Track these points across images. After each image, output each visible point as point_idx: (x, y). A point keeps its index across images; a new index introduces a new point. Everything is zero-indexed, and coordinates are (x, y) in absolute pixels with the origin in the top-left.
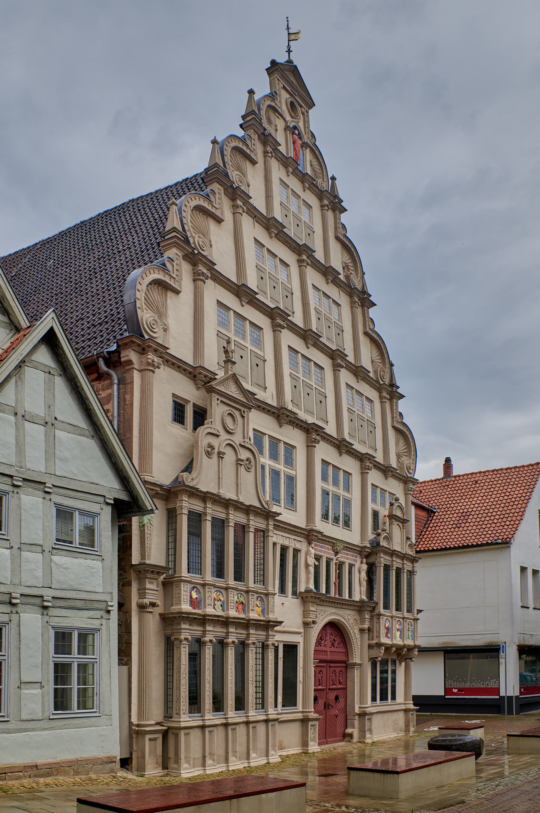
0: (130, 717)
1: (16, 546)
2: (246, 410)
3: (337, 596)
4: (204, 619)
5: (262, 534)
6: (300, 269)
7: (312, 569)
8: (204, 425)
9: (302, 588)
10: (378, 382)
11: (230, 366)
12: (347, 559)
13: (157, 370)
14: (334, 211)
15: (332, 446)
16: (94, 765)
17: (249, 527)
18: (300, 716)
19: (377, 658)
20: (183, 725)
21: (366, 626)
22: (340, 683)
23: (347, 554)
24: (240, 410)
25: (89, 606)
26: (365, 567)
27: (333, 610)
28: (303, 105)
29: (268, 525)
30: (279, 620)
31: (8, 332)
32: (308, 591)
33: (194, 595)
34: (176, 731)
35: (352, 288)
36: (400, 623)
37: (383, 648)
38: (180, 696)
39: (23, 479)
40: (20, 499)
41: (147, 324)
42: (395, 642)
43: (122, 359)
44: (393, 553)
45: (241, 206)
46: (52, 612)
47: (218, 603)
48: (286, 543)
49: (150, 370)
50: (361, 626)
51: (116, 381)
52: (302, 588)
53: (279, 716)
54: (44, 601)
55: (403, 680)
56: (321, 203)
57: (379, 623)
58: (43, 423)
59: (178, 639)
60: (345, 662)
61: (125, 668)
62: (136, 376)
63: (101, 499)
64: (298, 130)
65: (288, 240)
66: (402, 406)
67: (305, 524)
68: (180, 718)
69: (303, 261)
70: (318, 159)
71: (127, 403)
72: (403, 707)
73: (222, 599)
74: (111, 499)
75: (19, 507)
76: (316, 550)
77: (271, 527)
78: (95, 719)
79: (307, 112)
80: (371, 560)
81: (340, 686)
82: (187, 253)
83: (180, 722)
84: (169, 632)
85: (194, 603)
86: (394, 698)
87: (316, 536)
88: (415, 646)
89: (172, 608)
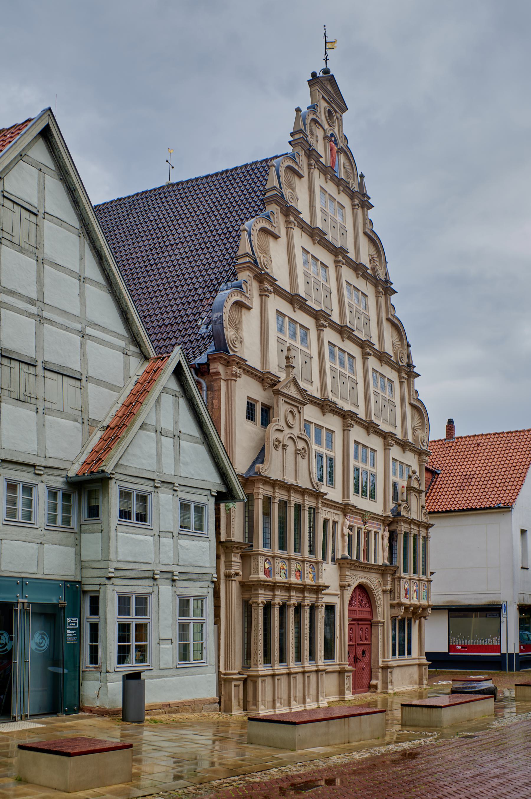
0: (219, 667)
1: (157, 534)
2: (302, 406)
3: (366, 562)
4: (274, 586)
5: (313, 511)
7: (346, 538)
10: (397, 363)
11: (291, 370)
12: (373, 527)
13: (238, 379)
14: (362, 207)
15: (362, 427)
17: (304, 507)
18: (337, 668)
19: (397, 617)
20: (261, 673)
21: (388, 588)
22: (366, 639)
23: (373, 523)
24: (297, 407)
25: (201, 578)
26: (387, 534)
27: (362, 574)
29: (317, 503)
31: (139, 360)
32: (344, 558)
33: (267, 567)
34: (254, 679)
35: (377, 280)
37: (403, 607)
38: (257, 649)
39: (161, 481)
40: (158, 497)
41: (231, 341)
42: (412, 602)
44: (411, 522)
45: (293, 222)
46: (179, 584)
48: (328, 517)
49: (233, 380)
50: (384, 588)
51: (205, 388)
52: (339, 556)
53: (326, 667)
54: (173, 575)
55: (417, 637)
56: (352, 202)
57: (400, 585)
58: (172, 436)
59: (256, 602)
60: (370, 620)
61: (216, 626)
62: (223, 384)
63: (208, 493)
64: (334, 137)
65: (328, 244)
66: (418, 384)
67: (341, 499)
68: (258, 667)
69: (339, 262)
70: (349, 159)
71: (215, 407)
72: (417, 662)
73: (285, 568)
74: (214, 492)
75: (158, 503)
76: (349, 521)
77: (320, 505)
78: (204, 668)
79: (341, 116)
80: (393, 528)
81: (366, 642)
82: (256, 273)
83: (258, 671)
84: (247, 597)
85: (267, 572)
86: (409, 653)
87: (351, 509)
88: (429, 606)
89: (251, 576)
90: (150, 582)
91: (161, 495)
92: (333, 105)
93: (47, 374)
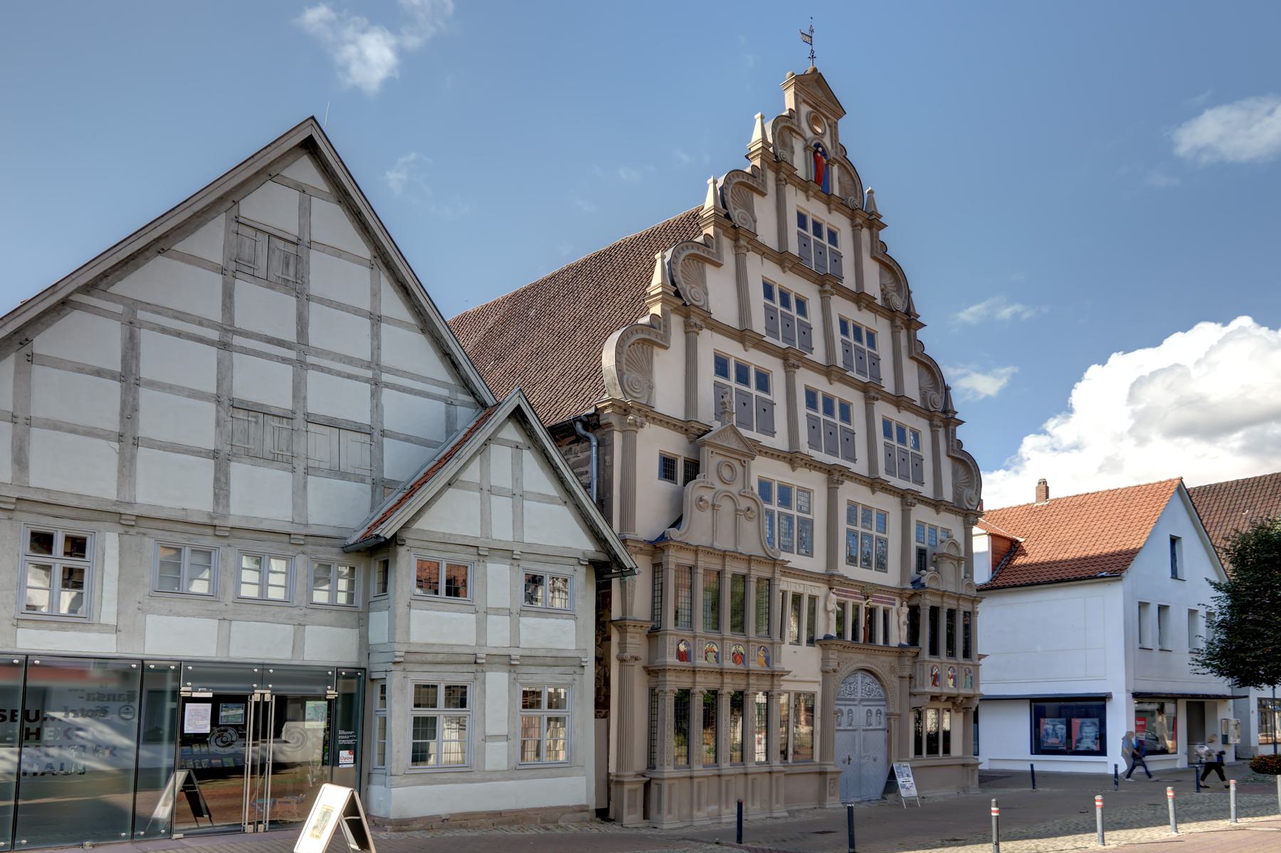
1: (481, 610)
2: (746, 459)
6: (822, 300)
8: (695, 479)
9: (820, 634)
11: (727, 418)
12: (882, 602)
14: (870, 228)
16: (563, 814)
17: (750, 577)
18: (817, 769)
20: (666, 775)
21: (906, 674)
26: (906, 610)
27: (862, 657)
28: (830, 116)
29: (774, 573)
30: (786, 670)
32: (827, 637)
35: (893, 311)
36: (954, 669)
38: (664, 747)
40: (485, 567)
42: (945, 690)
43: (601, 422)
45: (745, 246)
46: (520, 669)
47: (711, 655)
48: (799, 590)
49: (634, 431)
50: (900, 674)
52: (820, 634)
57: (924, 670)
59: (662, 691)
64: (822, 147)
68: (664, 769)
69: (826, 292)
75: (485, 574)
76: (838, 595)
79: (836, 123)
80: (914, 602)
82: (675, 306)
83: (663, 772)
84: (653, 685)
87: (838, 581)
89: (658, 660)
90: (474, 667)
91: (489, 565)
92: (823, 111)
93: (311, 427)
